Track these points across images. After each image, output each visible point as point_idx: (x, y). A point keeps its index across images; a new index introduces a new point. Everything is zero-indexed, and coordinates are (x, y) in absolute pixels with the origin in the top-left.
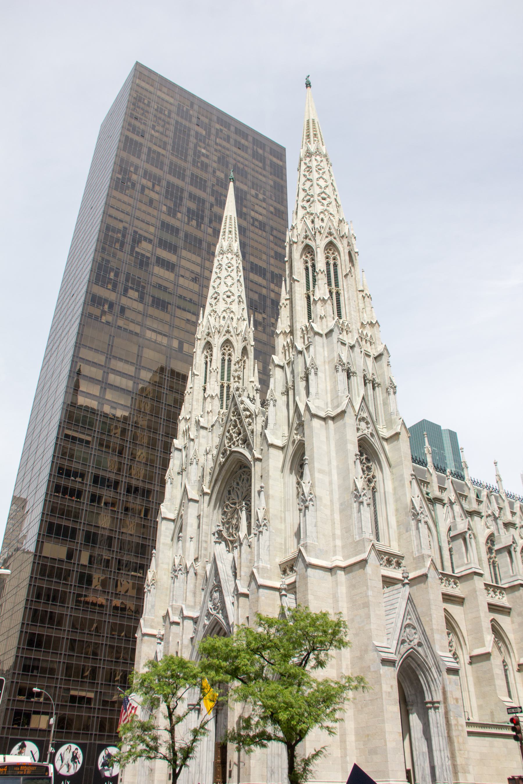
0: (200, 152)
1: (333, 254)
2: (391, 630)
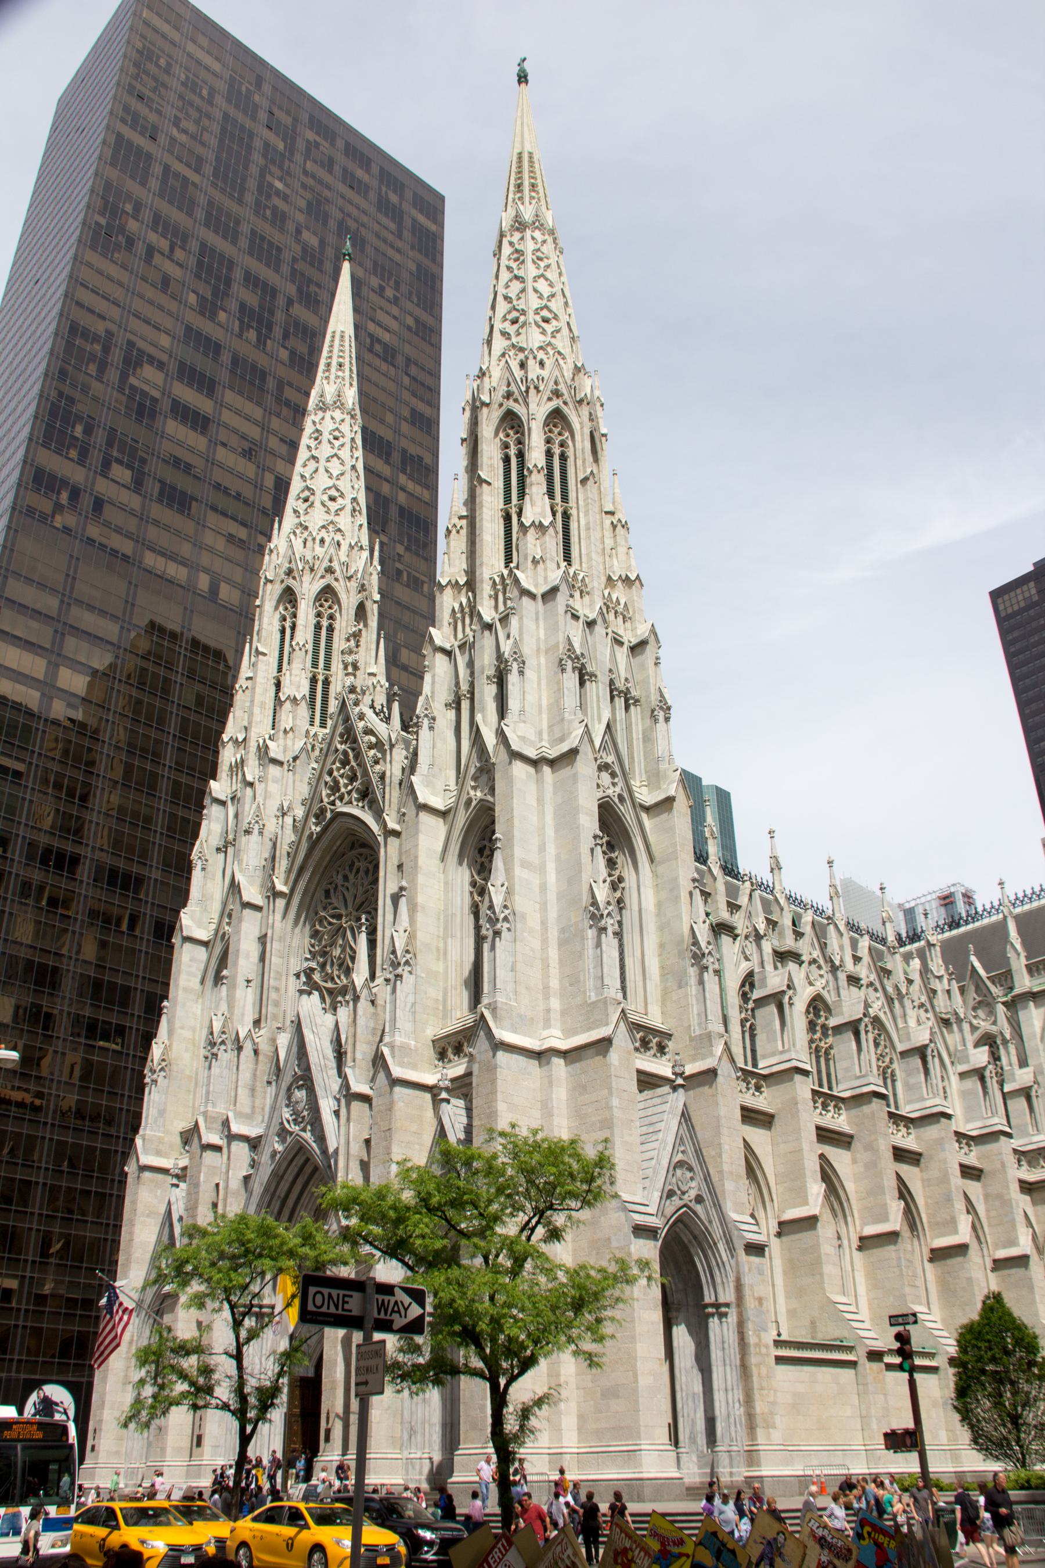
0: (271, 185)
1: (560, 434)
2: (649, 1172)
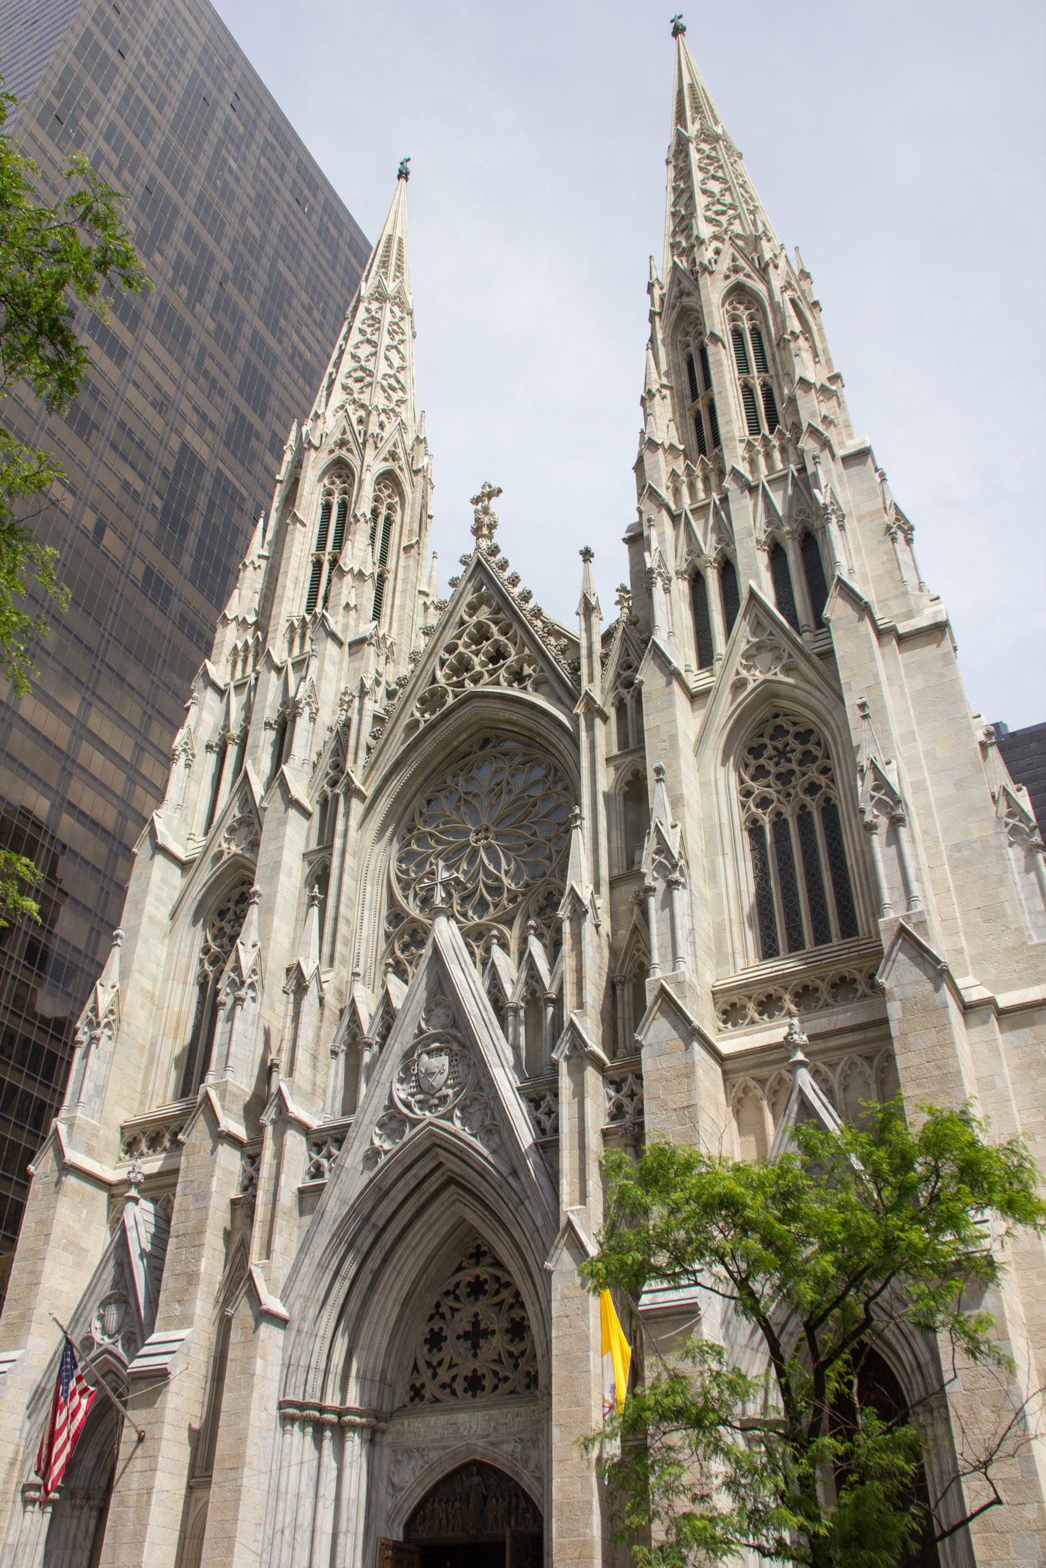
0: (225, 161)
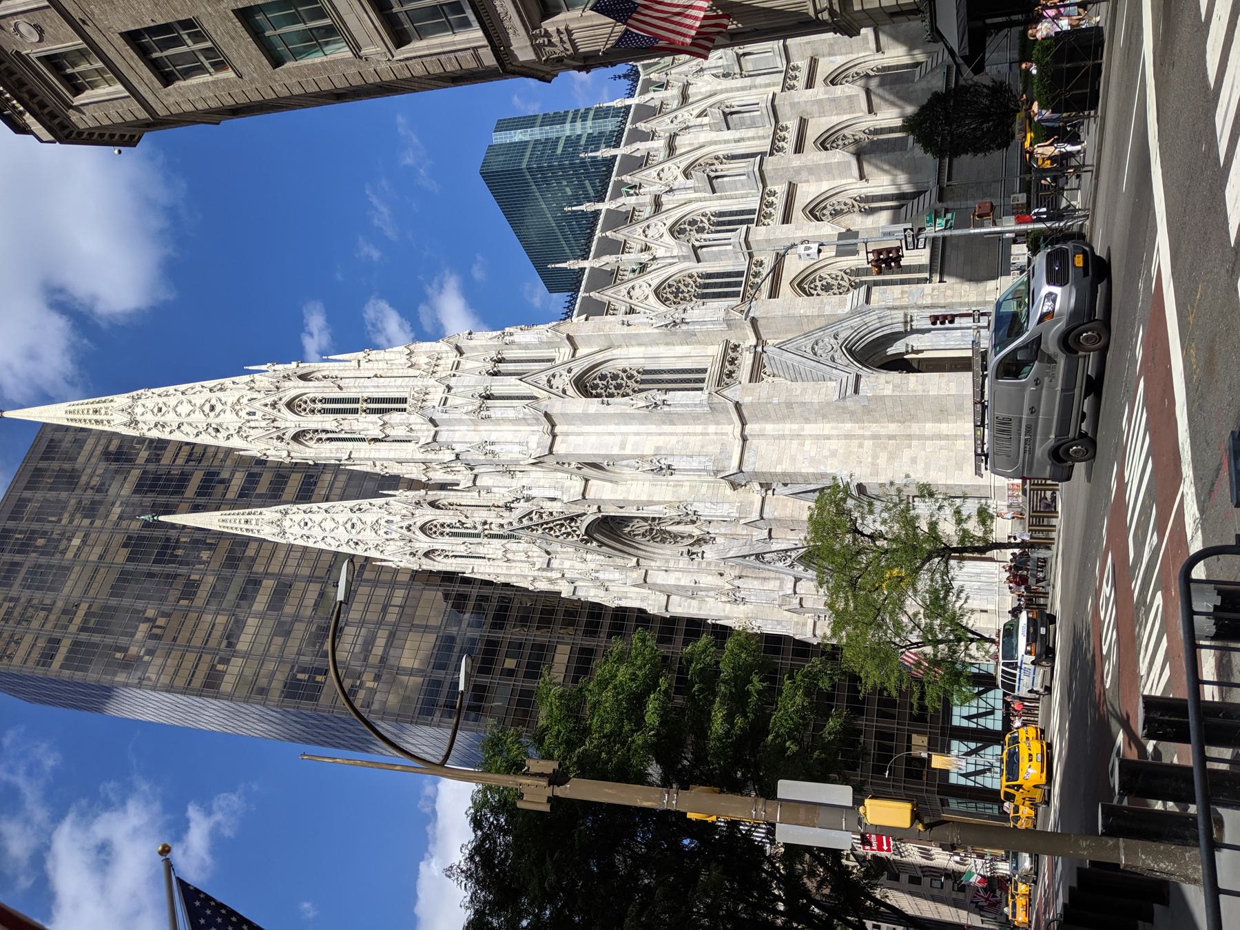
1: (306, 402)
